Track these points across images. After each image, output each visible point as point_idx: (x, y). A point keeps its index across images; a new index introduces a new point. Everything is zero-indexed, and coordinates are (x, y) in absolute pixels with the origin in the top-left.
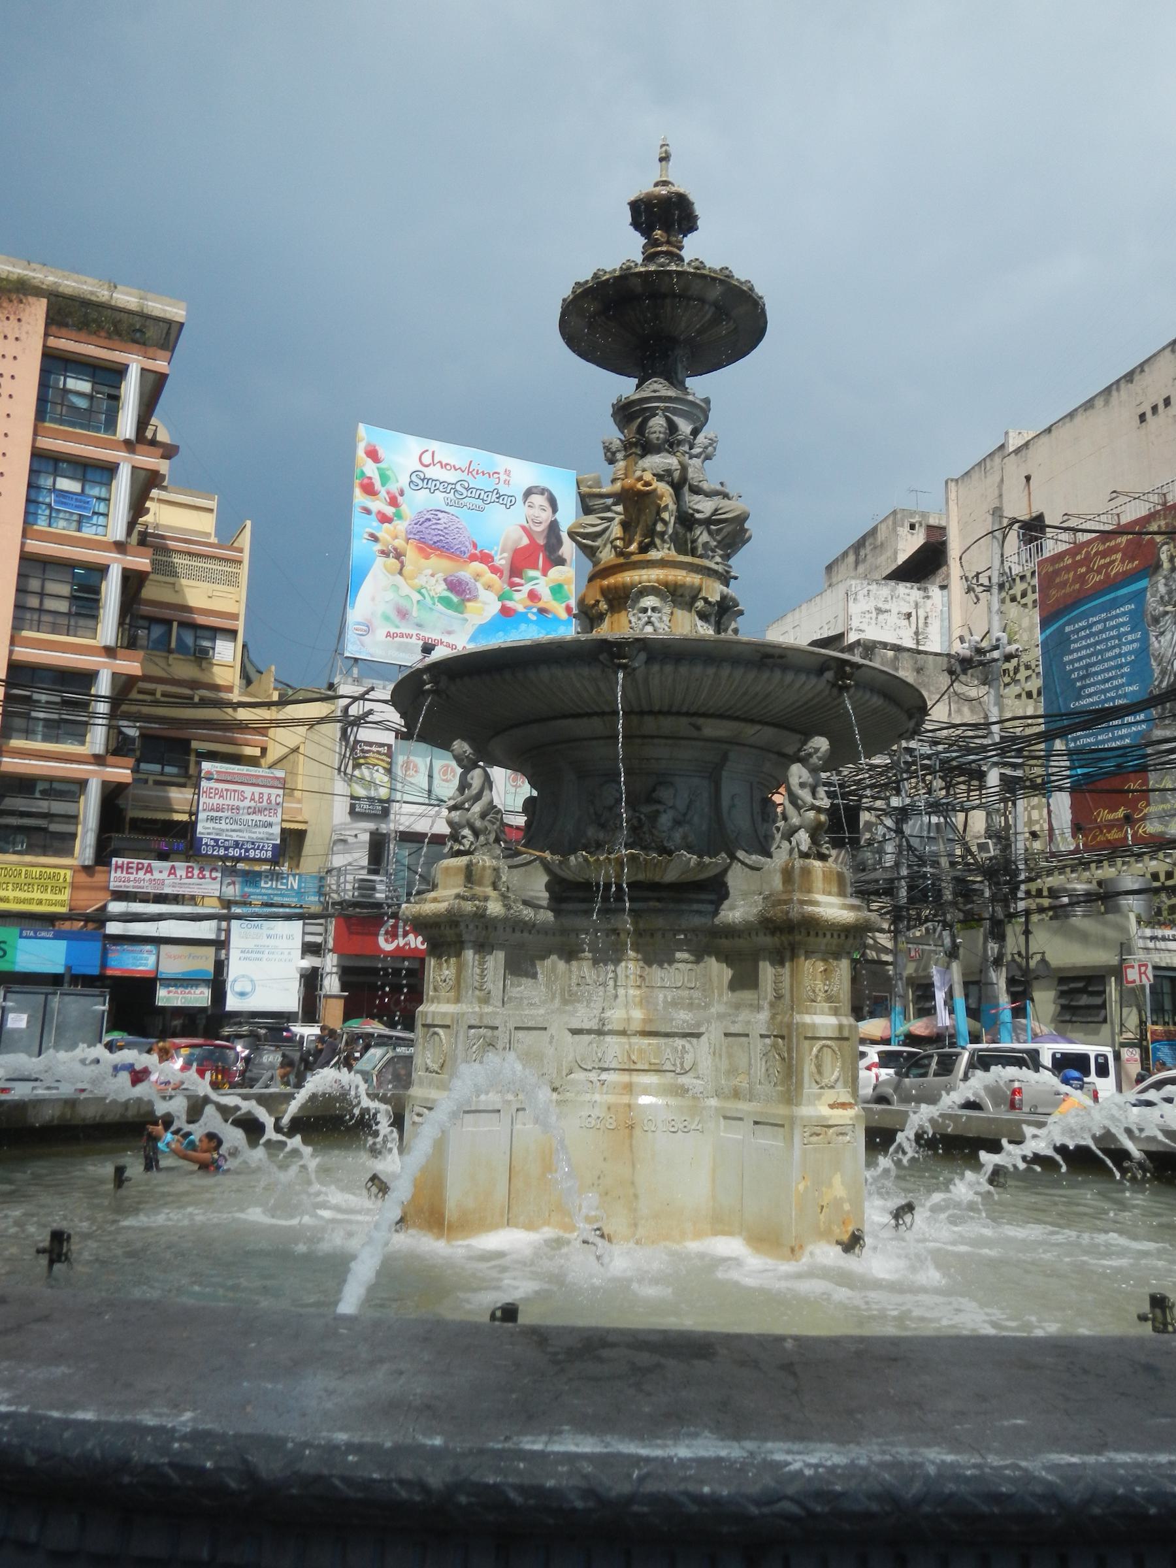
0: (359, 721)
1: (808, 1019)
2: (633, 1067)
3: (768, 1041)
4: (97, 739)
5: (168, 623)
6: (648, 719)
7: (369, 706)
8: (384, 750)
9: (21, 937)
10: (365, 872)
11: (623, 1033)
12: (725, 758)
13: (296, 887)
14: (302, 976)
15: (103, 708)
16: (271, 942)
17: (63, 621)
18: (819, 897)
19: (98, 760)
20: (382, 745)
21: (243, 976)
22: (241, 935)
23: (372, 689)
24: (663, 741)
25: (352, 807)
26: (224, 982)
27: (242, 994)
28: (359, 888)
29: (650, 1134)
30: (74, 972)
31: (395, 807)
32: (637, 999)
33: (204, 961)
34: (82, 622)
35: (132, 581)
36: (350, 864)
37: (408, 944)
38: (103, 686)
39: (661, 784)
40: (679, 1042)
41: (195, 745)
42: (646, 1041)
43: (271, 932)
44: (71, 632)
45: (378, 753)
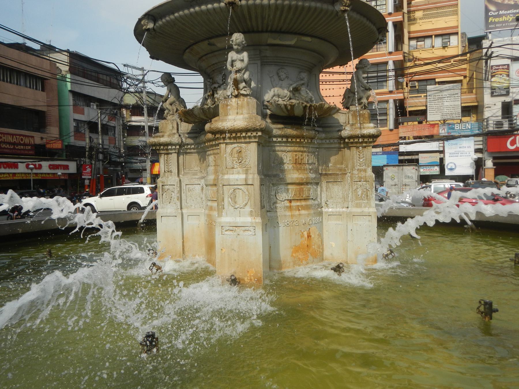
0: (490, 57)
5: (431, 37)
10: (500, 118)
13: (470, 128)
14: (475, 161)
16: (462, 149)
19: (391, 92)
20: (505, 65)
21: (451, 163)
22: (450, 147)
23: (492, 43)
24: (210, 55)
25: (492, 93)
26: (444, 165)
27: (451, 169)
28: (496, 124)
31: (511, 90)
33: (436, 158)
35: (398, 27)
38: (391, 66)
43: (461, 146)
45: (503, 69)
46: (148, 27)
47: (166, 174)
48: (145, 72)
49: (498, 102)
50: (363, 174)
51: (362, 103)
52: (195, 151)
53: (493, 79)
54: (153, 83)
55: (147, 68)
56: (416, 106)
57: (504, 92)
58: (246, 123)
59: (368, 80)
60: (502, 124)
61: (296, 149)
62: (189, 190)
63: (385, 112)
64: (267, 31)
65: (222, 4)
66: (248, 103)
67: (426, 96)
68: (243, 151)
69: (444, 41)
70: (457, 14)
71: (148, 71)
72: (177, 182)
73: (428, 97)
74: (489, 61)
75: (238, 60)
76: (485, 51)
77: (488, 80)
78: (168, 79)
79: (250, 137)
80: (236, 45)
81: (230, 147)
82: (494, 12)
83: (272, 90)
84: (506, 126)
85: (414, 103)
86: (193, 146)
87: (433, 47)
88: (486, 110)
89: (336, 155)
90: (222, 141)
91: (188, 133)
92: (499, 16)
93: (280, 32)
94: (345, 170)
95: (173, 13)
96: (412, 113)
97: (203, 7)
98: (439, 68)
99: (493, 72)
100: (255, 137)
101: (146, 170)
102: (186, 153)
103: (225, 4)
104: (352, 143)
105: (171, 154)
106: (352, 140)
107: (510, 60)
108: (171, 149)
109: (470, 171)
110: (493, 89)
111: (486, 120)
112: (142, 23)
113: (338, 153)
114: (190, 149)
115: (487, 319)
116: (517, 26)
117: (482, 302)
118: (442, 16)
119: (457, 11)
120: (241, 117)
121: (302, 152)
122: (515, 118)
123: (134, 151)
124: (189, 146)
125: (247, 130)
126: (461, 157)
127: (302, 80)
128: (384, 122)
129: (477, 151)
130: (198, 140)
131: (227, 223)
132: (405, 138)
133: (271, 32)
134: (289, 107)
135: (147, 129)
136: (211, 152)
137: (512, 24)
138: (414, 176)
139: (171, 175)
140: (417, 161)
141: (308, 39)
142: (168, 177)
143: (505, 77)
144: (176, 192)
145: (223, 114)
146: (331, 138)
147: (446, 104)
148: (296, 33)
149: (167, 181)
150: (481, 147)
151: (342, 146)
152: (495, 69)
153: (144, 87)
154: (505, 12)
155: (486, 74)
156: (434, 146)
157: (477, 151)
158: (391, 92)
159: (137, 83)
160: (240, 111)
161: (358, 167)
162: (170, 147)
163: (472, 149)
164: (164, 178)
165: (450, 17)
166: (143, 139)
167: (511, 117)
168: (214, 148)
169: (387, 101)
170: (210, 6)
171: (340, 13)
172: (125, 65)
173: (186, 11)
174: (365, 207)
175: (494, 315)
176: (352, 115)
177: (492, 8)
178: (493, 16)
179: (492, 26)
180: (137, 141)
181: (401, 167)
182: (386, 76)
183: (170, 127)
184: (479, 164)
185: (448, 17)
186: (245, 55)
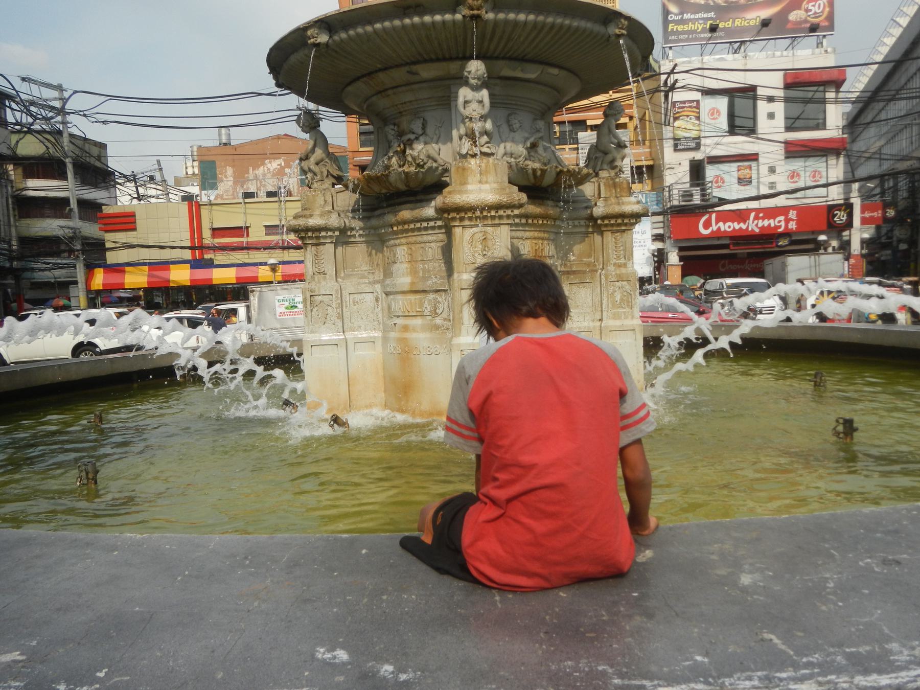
0: (673, 88)
6: (381, 75)
8: (694, 104)
10: (688, 185)
11: (403, 292)
20: (692, 101)
23: (676, 65)
24: (404, 88)
25: (676, 146)
28: (683, 196)
31: (703, 141)
36: (676, 183)
37: (719, 228)
40: (431, 296)
41: (589, 123)
42: (412, 297)
45: (690, 107)
46: (319, 40)
48: (66, 95)
49: (685, 158)
50: (623, 270)
51: (616, 166)
53: (677, 124)
54: (85, 115)
55: (69, 85)
57: (693, 145)
58: (497, 197)
60: (692, 195)
61: (536, 234)
64: (504, 58)
66: (495, 165)
67: (577, 149)
68: (489, 237)
71: (76, 92)
72: (337, 290)
73: (580, 151)
74: (670, 94)
75: (472, 101)
76: (663, 77)
78: (310, 123)
79: (500, 217)
80: (474, 78)
81: (469, 232)
82: (676, 15)
83: (502, 145)
84: (697, 200)
88: (667, 173)
89: (581, 242)
90: (457, 223)
91: (353, 211)
92: (682, 22)
93: (523, 59)
94: (595, 266)
95: (370, 23)
97: (427, 19)
100: (508, 217)
101: (76, 283)
102: (347, 243)
103: (464, 16)
104: (606, 225)
105: (324, 244)
106: (606, 222)
107: (700, 94)
108: (325, 237)
110: (676, 139)
112: (309, 33)
113: (584, 241)
115: (848, 440)
116: (710, 39)
117: (841, 421)
121: (542, 239)
122: (710, 185)
123: (51, 246)
125: (498, 207)
127: (538, 131)
129: (658, 238)
130: (374, 222)
133: (510, 59)
134: (539, 173)
135: (74, 205)
136: (403, 241)
137: (702, 36)
139: (325, 279)
141: (555, 71)
142: (319, 282)
143: (694, 121)
144: (334, 306)
145: (458, 182)
146: (576, 219)
148: (541, 63)
149: (319, 289)
150: (661, 231)
151: (590, 230)
152: (679, 108)
153: (64, 123)
154: (692, 16)
155: (666, 115)
157: (658, 238)
159: (51, 114)
160: (484, 179)
161: (615, 261)
162: (323, 234)
163: (648, 236)
164: (313, 284)
166: (62, 222)
167: (703, 184)
168: (410, 234)
170: (438, 18)
171: (613, 38)
172: (24, 79)
173: (397, 23)
174: (626, 318)
175: (855, 434)
176: (605, 184)
177: (673, 8)
180: (51, 226)
183: (320, 200)
184: (660, 259)
186: (485, 93)
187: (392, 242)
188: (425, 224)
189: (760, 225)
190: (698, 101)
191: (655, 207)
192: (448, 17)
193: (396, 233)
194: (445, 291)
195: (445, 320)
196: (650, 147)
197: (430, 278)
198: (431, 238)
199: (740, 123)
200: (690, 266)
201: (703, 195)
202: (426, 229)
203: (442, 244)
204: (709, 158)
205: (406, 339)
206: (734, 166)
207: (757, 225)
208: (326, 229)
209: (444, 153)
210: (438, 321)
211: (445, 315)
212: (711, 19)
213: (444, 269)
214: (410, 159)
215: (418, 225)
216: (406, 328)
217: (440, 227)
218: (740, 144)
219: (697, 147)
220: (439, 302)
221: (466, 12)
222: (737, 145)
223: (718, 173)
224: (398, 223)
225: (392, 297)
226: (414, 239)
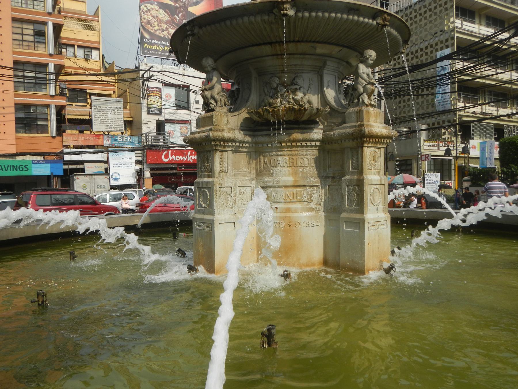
0: (149, 79)
1: (369, 177)
2: (289, 200)
3: (351, 187)
4: (52, 89)
5: (73, 46)
7: (151, 73)
9: (33, 163)
12: (325, 64)
15: (52, 77)
16: (124, 160)
17: (32, 44)
18: (372, 123)
19: (52, 97)
20: (158, 88)
22: (114, 158)
23: (152, 67)
24: (299, 56)
27: (116, 179)
28: (154, 139)
29: (298, 228)
30: (54, 174)
32: (291, 172)
33: (101, 167)
34: (39, 45)
35: (58, 28)
37: (173, 159)
39: (297, 76)
40: (309, 189)
41: (88, 91)
42: (294, 190)
44: (36, 49)
45: (156, 91)
47: (221, 174)
52: (247, 150)
56: (73, 115)
57: (158, 112)
59: (24, 79)
60: (159, 140)
62: (241, 193)
63: (46, 117)
65: (375, 23)
68: (376, 154)
69: (86, 53)
70: (98, 30)
73: (93, 108)
76: (142, 72)
77: (145, 99)
84: (161, 142)
85: (75, 111)
86: (247, 145)
87: (76, 57)
88: (144, 126)
90: (366, 145)
92: (151, 44)
96: (71, 121)
97: (361, 19)
98: (104, 81)
99: (148, 93)
105: (226, 151)
109: (132, 181)
111: (144, 135)
114: (243, 147)
116: (169, 56)
118: (85, 29)
119: (98, 27)
120: (378, 124)
124: (244, 145)
125: (384, 137)
126: (124, 168)
128: (44, 129)
131: (373, 219)
132: (67, 147)
137: (162, 54)
138: (106, 185)
139: (226, 176)
140: (83, 170)
143: (158, 99)
147: (110, 116)
149: (224, 182)
150: (140, 159)
152: (151, 91)
154: (157, 42)
156: (100, 157)
157: (138, 162)
158: (52, 97)
162: (230, 144)
163: (134, 161)
165: (93, 32)
169: (48, 106)
170: (366, 20)
173: (345, 16)
177: (146, 35)
178: (147, 43)
179: (147, 52)
181: (93, 176)
182: (46, 78)
183: (225, 120)
184: (140, 174)
185: (91, 32)
187: (274, 153)
188: (309, 144)
189: (193, 158)
190: (160, 89)
191: (138, 144)
192: (371, 21)
193: (282, 147)
194: (317, 186)
195: (316, 204)
196: (130, 110)
197: (307, 178)
198: (308, 152)
199: (183, 104)
200: (157, 178)
201: (164, 140)
202: (307, 146)
203: (314, 157)
204: (166, 120)
205: (290, 217)
206: (179, 125)
207: (191, 158)
208: (233, 141)
209: (315, 100)
210: (312, 205)
211: (316, 202)
212: (166, 46)
213: (316, 172)
214: (291, 101)
215: (304, 144)
216: (288, 210)
217: (316, 146)
218: (183, 114)
219: (160, 113)
220: (313, 193)
221: (380, 21)
222: (180, 115)
223: (172, 129)
224: (290, 141)
225: (272, 189)
226: (296, 152)
